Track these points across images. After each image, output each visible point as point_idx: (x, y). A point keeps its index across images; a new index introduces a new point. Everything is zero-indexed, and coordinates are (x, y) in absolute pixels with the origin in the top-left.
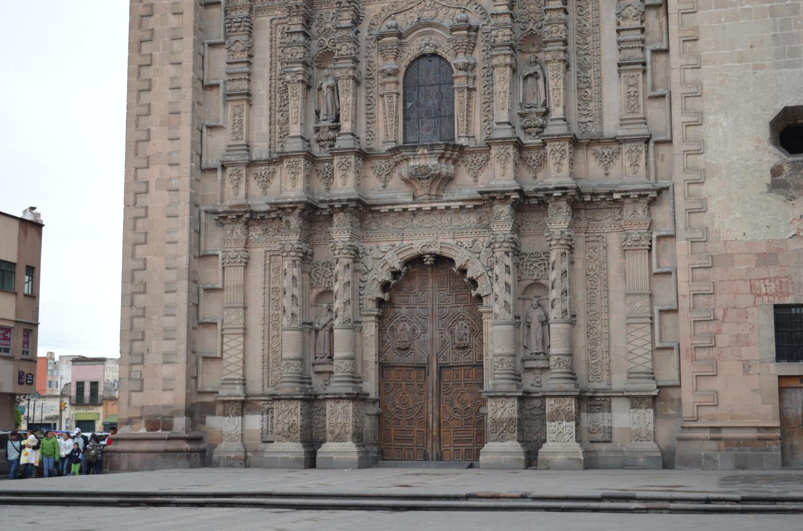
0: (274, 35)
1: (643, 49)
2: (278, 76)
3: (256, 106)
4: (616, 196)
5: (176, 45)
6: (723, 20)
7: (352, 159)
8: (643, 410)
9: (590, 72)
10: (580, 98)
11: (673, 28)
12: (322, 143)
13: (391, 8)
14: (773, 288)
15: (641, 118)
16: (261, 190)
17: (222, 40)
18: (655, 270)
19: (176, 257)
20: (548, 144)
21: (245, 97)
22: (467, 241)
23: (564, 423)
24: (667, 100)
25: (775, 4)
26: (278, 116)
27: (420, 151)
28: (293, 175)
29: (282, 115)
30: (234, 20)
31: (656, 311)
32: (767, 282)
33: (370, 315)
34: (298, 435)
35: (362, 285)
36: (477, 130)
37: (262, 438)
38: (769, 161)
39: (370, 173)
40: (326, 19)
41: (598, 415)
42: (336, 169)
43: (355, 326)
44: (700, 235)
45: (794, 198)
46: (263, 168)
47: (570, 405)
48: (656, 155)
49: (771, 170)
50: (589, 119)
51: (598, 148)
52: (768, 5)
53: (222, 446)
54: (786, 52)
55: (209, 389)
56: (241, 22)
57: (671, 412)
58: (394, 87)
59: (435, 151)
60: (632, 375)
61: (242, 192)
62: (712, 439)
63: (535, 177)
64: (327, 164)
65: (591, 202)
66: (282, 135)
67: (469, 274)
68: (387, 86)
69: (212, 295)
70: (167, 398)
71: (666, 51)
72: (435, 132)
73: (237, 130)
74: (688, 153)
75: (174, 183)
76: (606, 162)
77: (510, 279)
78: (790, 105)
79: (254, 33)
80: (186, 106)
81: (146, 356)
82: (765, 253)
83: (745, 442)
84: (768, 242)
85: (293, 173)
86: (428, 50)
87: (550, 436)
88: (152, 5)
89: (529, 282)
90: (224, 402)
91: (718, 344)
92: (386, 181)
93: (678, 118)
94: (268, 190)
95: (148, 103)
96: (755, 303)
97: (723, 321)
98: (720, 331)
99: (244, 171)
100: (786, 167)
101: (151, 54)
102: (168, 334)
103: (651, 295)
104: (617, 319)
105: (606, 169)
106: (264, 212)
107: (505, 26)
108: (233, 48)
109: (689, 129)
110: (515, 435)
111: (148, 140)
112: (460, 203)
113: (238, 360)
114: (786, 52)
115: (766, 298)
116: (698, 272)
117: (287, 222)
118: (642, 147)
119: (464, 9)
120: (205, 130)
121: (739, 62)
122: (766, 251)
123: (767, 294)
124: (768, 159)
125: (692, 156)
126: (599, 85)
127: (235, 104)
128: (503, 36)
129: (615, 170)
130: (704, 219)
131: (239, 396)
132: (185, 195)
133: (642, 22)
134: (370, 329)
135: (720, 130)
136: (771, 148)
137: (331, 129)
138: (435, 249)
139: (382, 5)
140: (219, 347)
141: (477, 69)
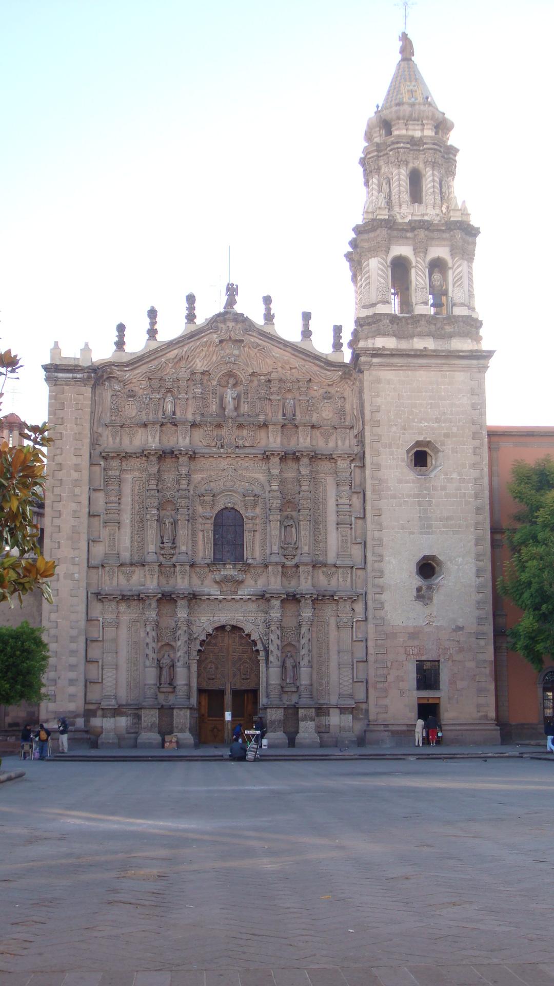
0: (134, 488)
1: (351, 516)
2: (136, 512)
3: (122, 530)
4: (336, 598)
5: (77, 490)
7: (188, 568)
8: (347, 715)
9: (321, 526)
10: (315, 540)
11: (368, 508)
12: (164, 556)
13: (207, 478)
14: (416, 651)
15: (348, 555)
16: (126, 582)
17: (102, 488)
18: (354, 640)
19: (77, 622)
20: (300, 567)
21: (117, 524)
22: (251, 618)
23: (309, 722)
26: (136, 537)
28: (151, 576)
30: (112, 477)
31: (355, 662)
33: (194, 660)
34: (157, 729)
36: (257, 554)
37: (127, 731)
39: (194, 575)
40: (167, 481)
41: (322, 717)
42: (178, 574)
44: (380, 621)
45: (427, 604)
46: (128, 569)
47: (312, 712)
48: (356, 575)
49: (417, 589)
51: (325, 569)
53: (103, 736)
55: (94, 702)
57: (361, 716)
58: (209, 526)
59: (237, 567)
61: (115, 583)
62: (385, 731)
63: (290, 584)
64: (168, 569)
65: (322, 600)
66: (139, 549)
67: (252, 638)
68: (206, 525)
69: (95, 644)
70: (72, 707)
71: (364, 518)
72: (232, 554)
76: (329, 576)
77: (279, 642)
79: (121, 487)
80: (84, 529)
81: (58, 681)
82: (412, 633)
83: (403, 732)
84: (414, 627)
86: (230, 505)
87: (301, 729)
88: (61, 464)
89: (286, 643)
90: (103, 709)
91: (389, 681)
92: (203, 581)
94: (130, 582)
95: (58, 525)
97: (390, 669)
98: (389, 674)
99: (116, 570)
101: (60, 495)
102: (72, 667)
103: (352, 653)
104: (333, 664)
105: (329, 581)
106: (129, 596)
107: (278, 498)
108: (110, 494)
110: (282, 729)
111: (59, 547)
112: (249, 597)
113: (112, 684)
115: (412, 656)
116: (379, 642)
117: (150, 604)
118: (349, 570)
120: (91, 542)
122: (412, 631)
123: (413, 654)
126: (326, 534)
127: (110, 528)
128: (277, 503)
129: (334, 582)
130: (381, 613)
131: (114, 706)
132: (83, 584)
133: (350, 500)
134: (194, 667)
135: (392, 565)
136: (417, 577)
137: (172, 548)
140: (100, 676)
141: (258, 519)
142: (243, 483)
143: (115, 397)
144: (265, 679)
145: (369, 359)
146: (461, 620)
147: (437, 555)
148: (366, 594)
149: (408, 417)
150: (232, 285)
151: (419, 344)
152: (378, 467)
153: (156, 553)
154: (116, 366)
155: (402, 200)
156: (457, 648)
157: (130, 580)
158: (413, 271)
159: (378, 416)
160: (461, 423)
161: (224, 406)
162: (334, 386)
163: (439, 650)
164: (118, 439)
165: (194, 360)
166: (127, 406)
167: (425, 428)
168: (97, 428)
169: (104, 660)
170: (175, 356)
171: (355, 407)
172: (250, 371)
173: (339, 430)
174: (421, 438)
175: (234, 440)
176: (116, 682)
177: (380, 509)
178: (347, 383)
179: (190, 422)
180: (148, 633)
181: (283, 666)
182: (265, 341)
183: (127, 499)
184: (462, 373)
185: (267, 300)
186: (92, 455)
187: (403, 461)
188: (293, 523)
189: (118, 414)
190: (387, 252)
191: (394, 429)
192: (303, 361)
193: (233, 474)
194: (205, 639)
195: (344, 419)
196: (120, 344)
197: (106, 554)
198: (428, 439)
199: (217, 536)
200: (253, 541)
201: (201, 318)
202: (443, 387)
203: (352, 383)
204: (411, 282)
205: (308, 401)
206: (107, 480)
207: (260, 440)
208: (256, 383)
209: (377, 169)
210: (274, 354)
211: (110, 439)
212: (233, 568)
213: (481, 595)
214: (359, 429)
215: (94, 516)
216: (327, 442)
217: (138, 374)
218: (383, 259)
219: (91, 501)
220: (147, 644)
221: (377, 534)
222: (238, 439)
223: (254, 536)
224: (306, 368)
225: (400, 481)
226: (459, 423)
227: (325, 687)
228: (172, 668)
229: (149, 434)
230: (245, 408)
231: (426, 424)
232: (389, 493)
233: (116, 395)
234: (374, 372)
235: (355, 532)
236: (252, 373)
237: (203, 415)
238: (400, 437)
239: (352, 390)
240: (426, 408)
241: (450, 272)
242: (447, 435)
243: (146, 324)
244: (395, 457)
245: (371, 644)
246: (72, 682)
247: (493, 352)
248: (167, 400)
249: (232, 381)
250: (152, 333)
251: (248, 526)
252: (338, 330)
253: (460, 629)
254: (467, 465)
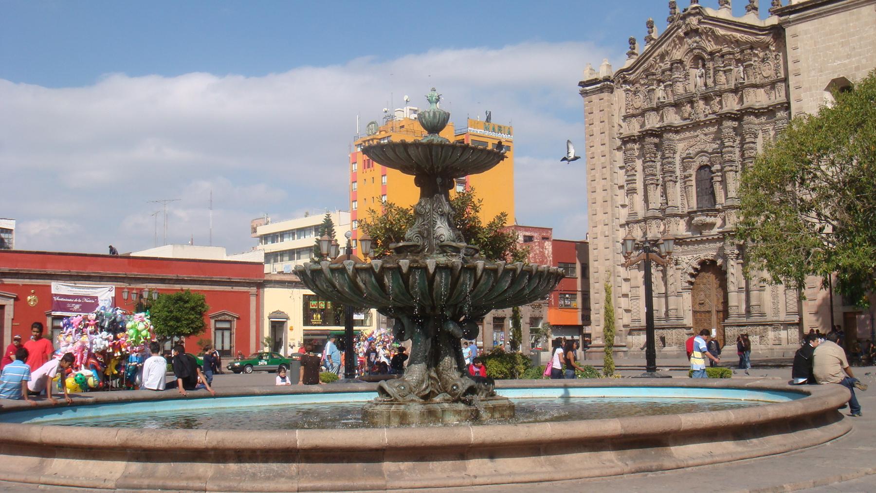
60: (788, 313)
75: (607, 233)
154: (626, 72)
160: (869, 54)
174: (835, 77)
178: (781, 41)
184: (867, 7)
198: (841, 76)
202: (851, 24)
226: (867, 54)
238: (818, 80)
244: (815, 98)
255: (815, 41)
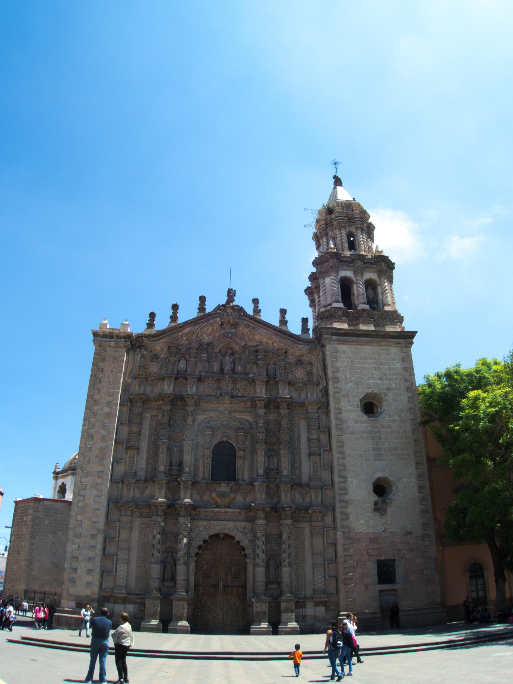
0: (152, 423)
2: (152, 442)
6: (353, 439)
8: (321, 607)
9: (296, 457)
13: (208, 419)
24: (330, 471)
25: (373, 435)
26: (151, 461)
27: (222, 485)
28: (160, 490)
29: (153, 461)
32: (374, 550)
33: (193, 560)
35: (189, 545)
38: (373, 499)
39: (195, 492)
41: (300, 609)
43: (186, 564)
45: (383, 515)
46: (142, 485)
47: (292, 605)
48: (325, 494)
50: (296, 477)
52: (370, 435)
54: (378, 454)
56: (138, 415)
67: (241, 544)
73: (131, 465)
74: (340, 494)
77: (264, 547)
78: (380, 476)
79: (142, 421)
82: (373, 538)
85: (160, 489)
86: (225, 439)
93: (337, 479)
96: (369, 559)
100: (380, 502)
104: (308, 567)
109: (341, 484)
114: (378, 454)
115: (373, 557)
116: (346, 546)
119: (242, 423)
121: (360, 457)
122: (373, 537)
124: (372, 498)
125: (343, 496)
134: (192, 566)
135: (354, 485)
136: (374, 494)
138: (226, 531)
139: (204, 417)
140: (114, 569)
142: (236, 423)
143: (143, 358)
144: (252, 578)
145: (330, 336)
146: (409, 526)
147: (388, 477)
148: (334, 509)
149: (360, 377)
150: (232, 290)
151: (363, 327)
152: (339, 411)
153: (165, 473)
154: (146, 337)
155: (344, 246)
156: (408, 549)
157: (143, 494)
158: (355, 286)
159: (338, 375)
161: (223, 367)
162: (304, 356)
163: (394, 551)
164: (143, 388)
165: (203, 335)
166: (151, 365)
167: (372, 384)
168: (128, 380)
169: (119, 557)
170: (189, 331)
171: (320, 370)
172: (243, 344)
173: (309, 386)
174: (370, 391)
175: (229, 391)
176: (127, 575)
177: (342, 442)
179: (197, 376)
180: (154, 536)
181: (267, 566)
182: (254, 324)
183: (146, 430)
184: (395, 348)
185: (256, 301)
186: (122, 398)
187: (357, 407)
188: (275, 454)
189: (144, 370)
190: (337, 273)
191: (350, 384)
192: (282, 338)
193: (228, 416)
194: (202, 544)
195: (312, 378)
196: (151, 325)
197: (126, 472)
198: (375, 392)
199: (214, 463)
200: (243, 467)
201: (210, 308)
203: (317, 354)
204: (353, 294)
205: (285, 366)
206: (131, 416)
207: (249, 392)
208: (247, 352)
209: (325, 234)
210: (260, 332)
211: (137, 387)
212: (227, 487)
213: (423, 506)
214: (323, 385)
215: (119, 443)
216: (299, 395)
217: (162, 342)
218: (334, 276)
219: (118, 431)
220: (153, 545)
221: (341, 461)
222: (233, 391)
223: (244, 463)
224: (284, 342)
225: (356, 422)
226: (396, 381)
227: (302, 584)
228: (174, 566)
229: (165, 384)
230: (239, 368)
231: (373, 381)
232: (349, 430)
233: (144, 357)
234: (333, 346)
235: (324, 460)
236: (244, 345)
237: (207, 372)
238: (354, 390)
239: (317, 359)
240: (372, 370)
241: (379, 288)
242: (388, 389)
243: (170, 312)
244: (352, 404)
245: (340, 548)
246: (89, 572)
247: (416, 332)
248: (181, 362)
249: (229, 351)
250: (174, 318)
251: (240, 454)
252: (305, 321)
253: (409, 533)
254: (405, 410)
255: (352, 361)
